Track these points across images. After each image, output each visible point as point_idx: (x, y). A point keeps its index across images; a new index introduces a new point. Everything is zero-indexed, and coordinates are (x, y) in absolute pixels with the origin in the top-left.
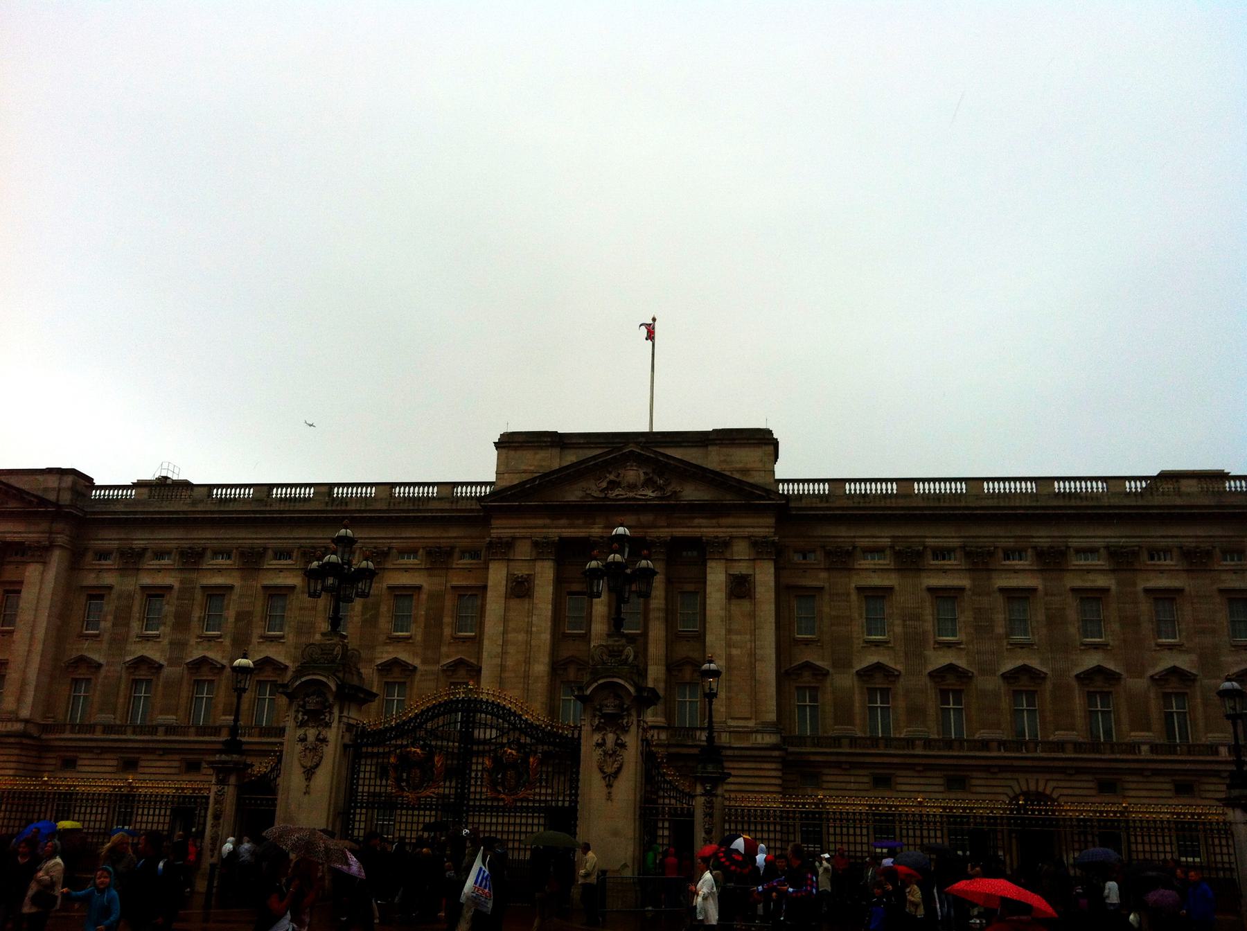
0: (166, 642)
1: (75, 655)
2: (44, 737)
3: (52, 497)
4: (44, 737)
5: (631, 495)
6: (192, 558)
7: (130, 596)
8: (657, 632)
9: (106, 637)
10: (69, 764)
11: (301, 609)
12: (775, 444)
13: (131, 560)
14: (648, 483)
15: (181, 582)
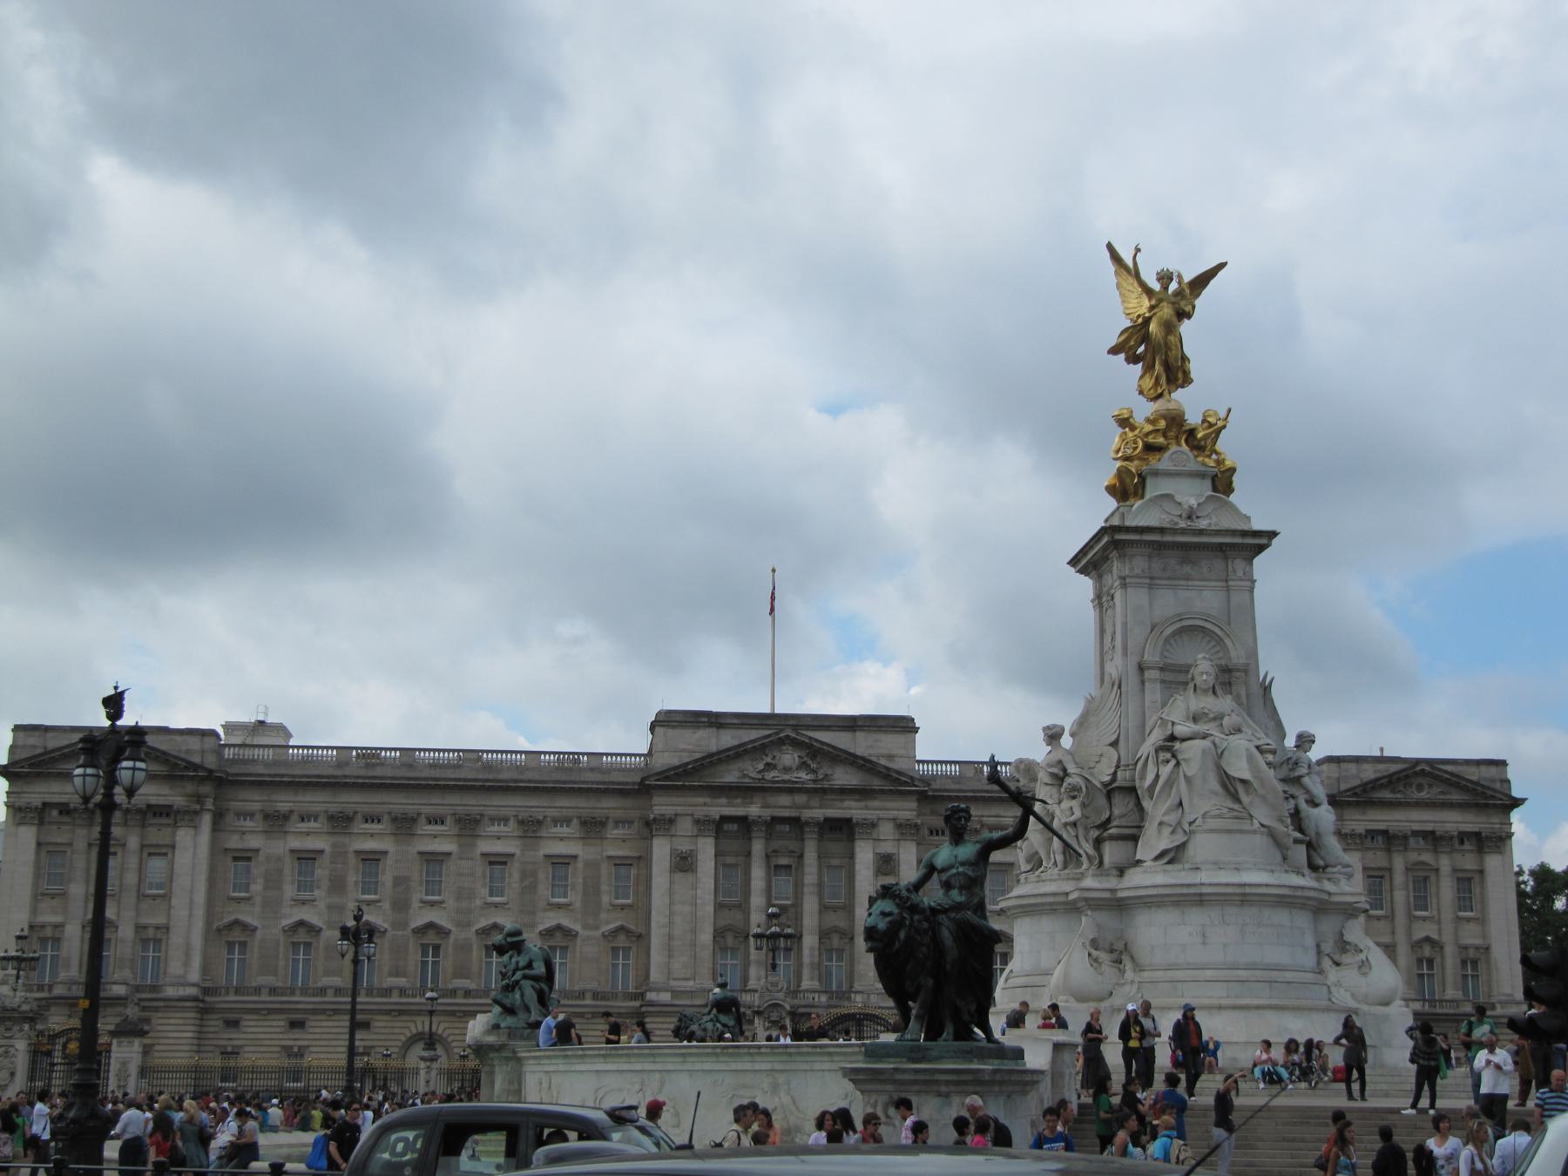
0: (322, 905)
1: (228, 919)
2: (208, 999)
3: (196, 759)
4: (208, 999)
5: (786, 777)
6: (340, 822)
7: (279, 859)
8: (810, 905)
9: (258, 899)
10: (233, 1024)
11: (460, 875)
12: (916, 730)
13: (276, 821)
14: (803, 765)
15: (334, 845)
